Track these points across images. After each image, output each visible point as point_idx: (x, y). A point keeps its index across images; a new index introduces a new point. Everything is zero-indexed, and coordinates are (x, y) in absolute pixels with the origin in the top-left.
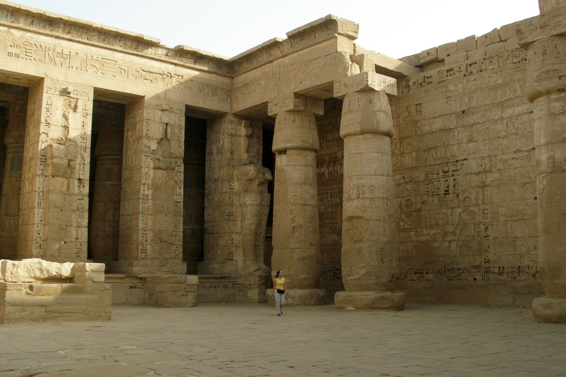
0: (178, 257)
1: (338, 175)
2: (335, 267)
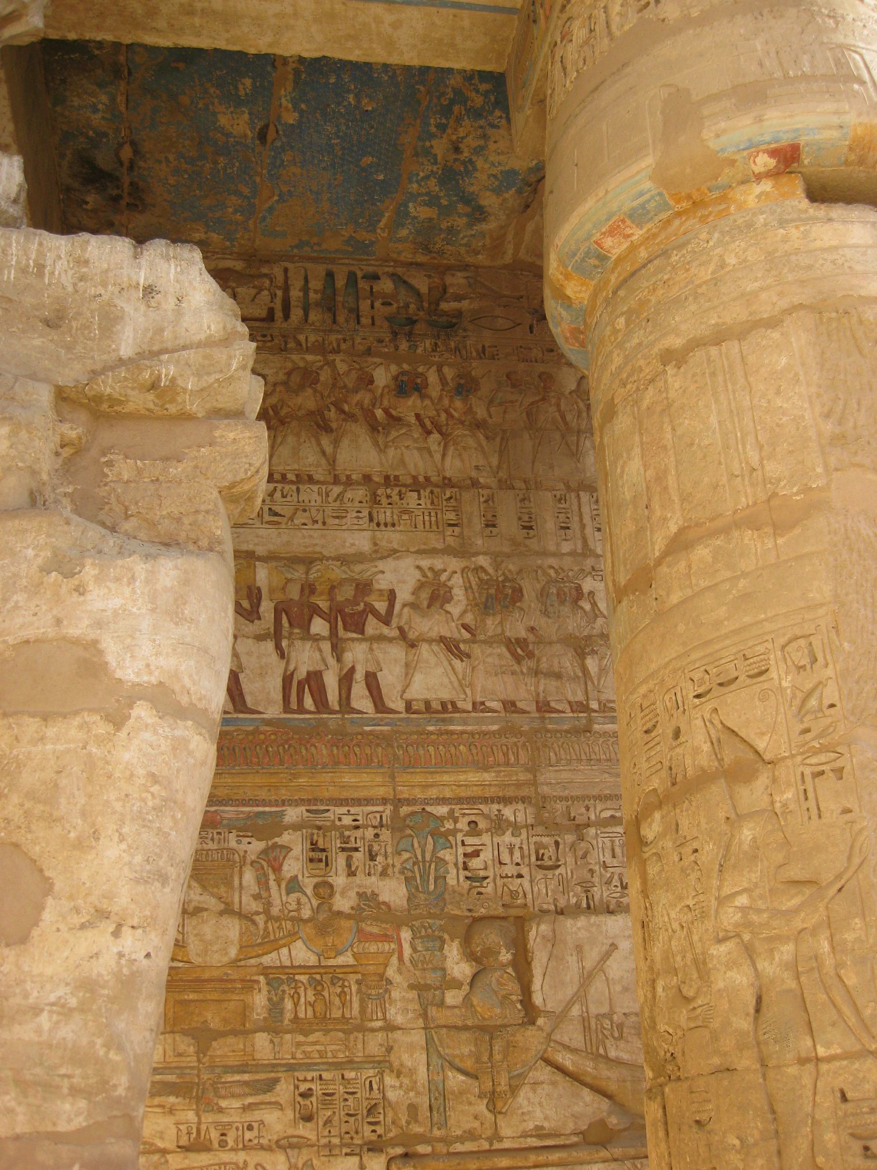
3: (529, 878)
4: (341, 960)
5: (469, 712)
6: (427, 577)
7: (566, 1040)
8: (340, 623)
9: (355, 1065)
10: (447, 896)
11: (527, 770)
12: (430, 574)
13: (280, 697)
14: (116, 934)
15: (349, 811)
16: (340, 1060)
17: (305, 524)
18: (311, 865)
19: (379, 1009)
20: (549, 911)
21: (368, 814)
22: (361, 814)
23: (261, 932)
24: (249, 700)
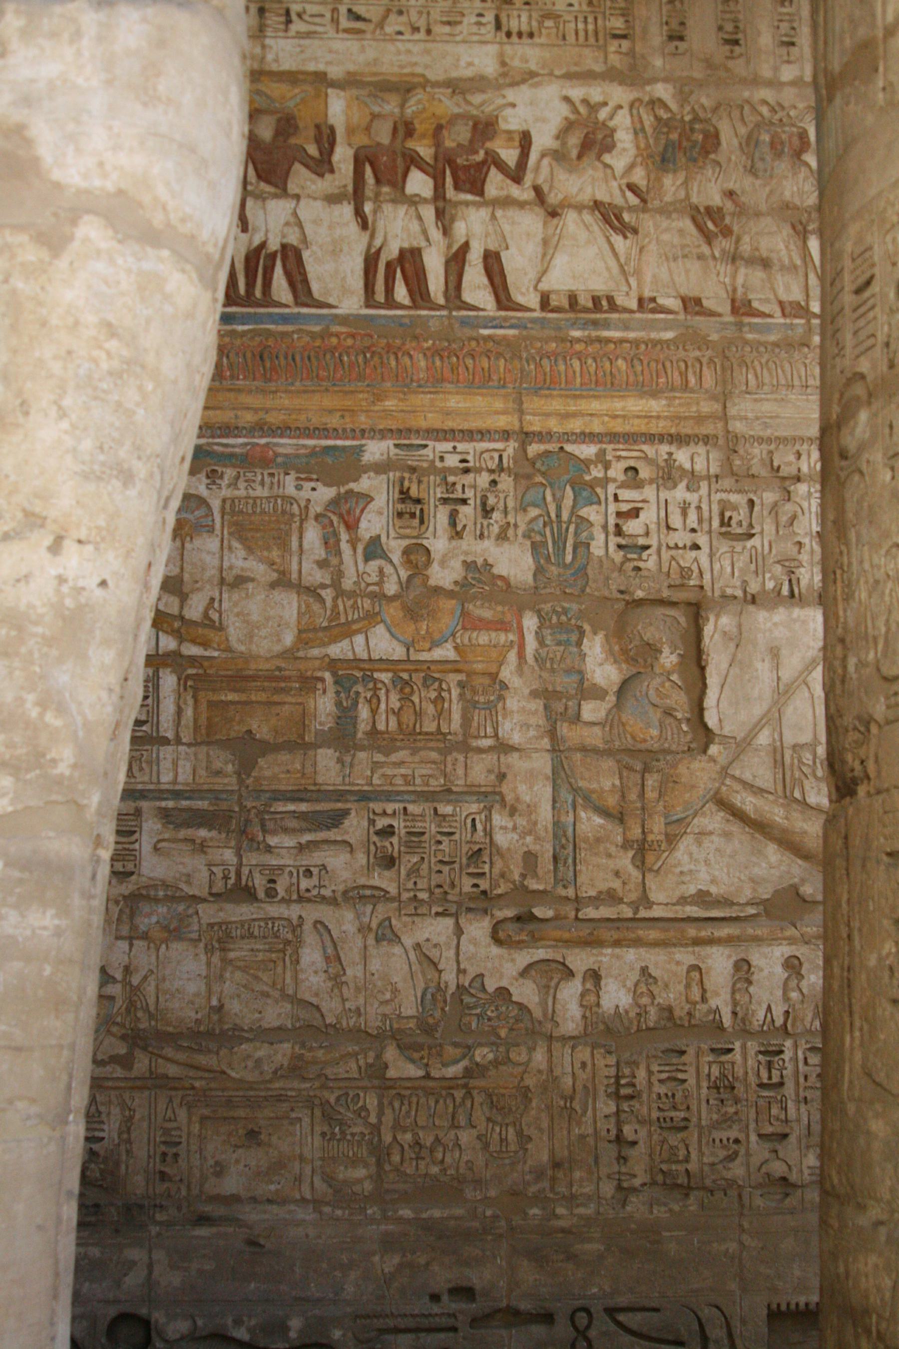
2: (465, 1292)
3: (707, 550)
4: (438, 654)
5: (631, 311)
6: (578, 113)
7: (747, 776)
8: (449, 180)
9: (453, 797)
10: (590, 571)
11: (714, 398)
12: (582, 110)
13: (361, 284)
14: (56, 548)
15: (455, 448)
16: (431, 789)
17: (400, 33)
18: (398, 523)
19: (489, 723)
20: (735, 597)
21: (482, 453)
22: (472, 452)
23: (329, 612)
24: (315, 287)
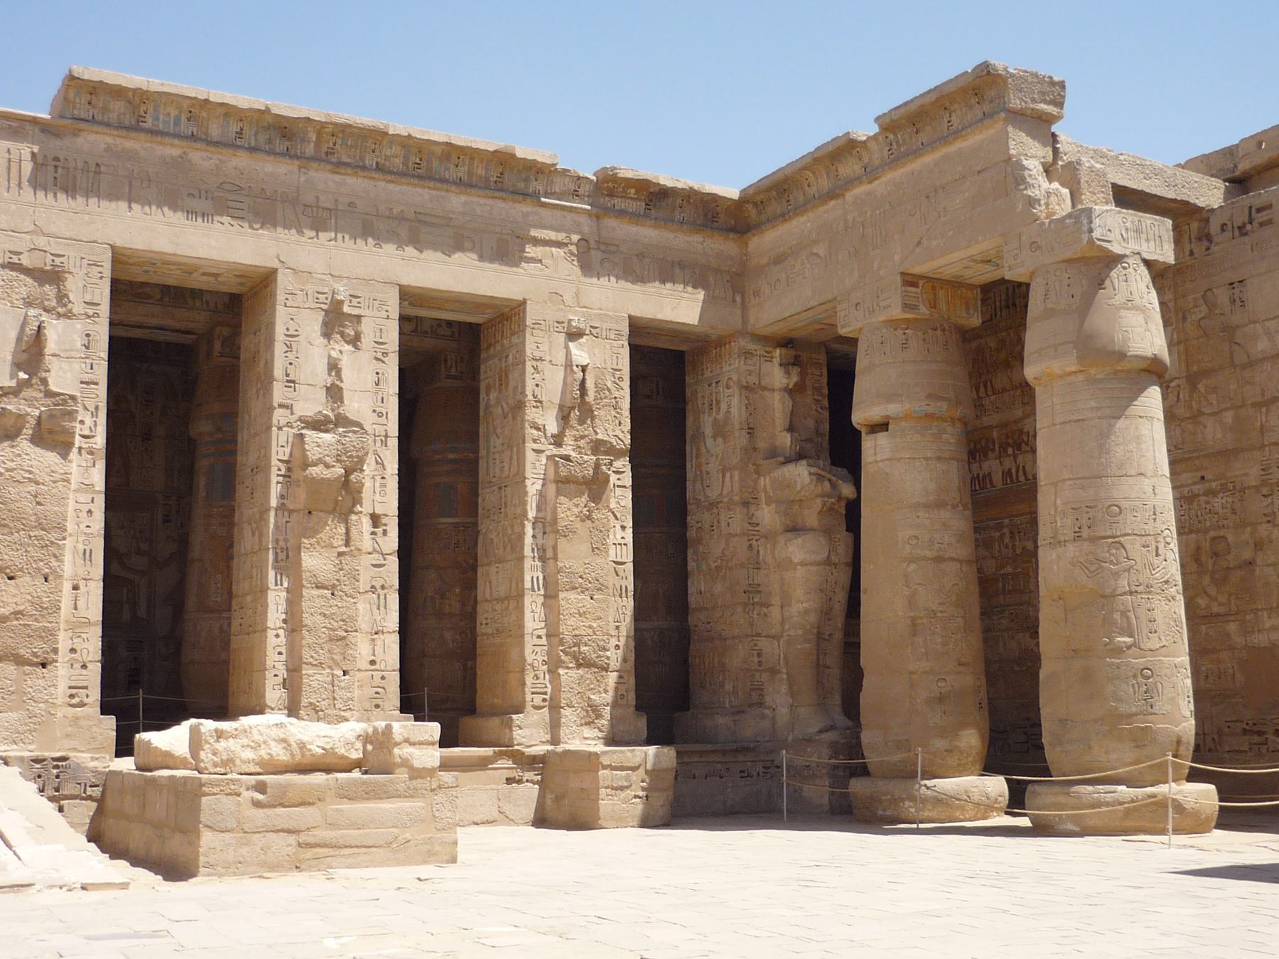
0: (624, 702)
1: (1027, 479)
